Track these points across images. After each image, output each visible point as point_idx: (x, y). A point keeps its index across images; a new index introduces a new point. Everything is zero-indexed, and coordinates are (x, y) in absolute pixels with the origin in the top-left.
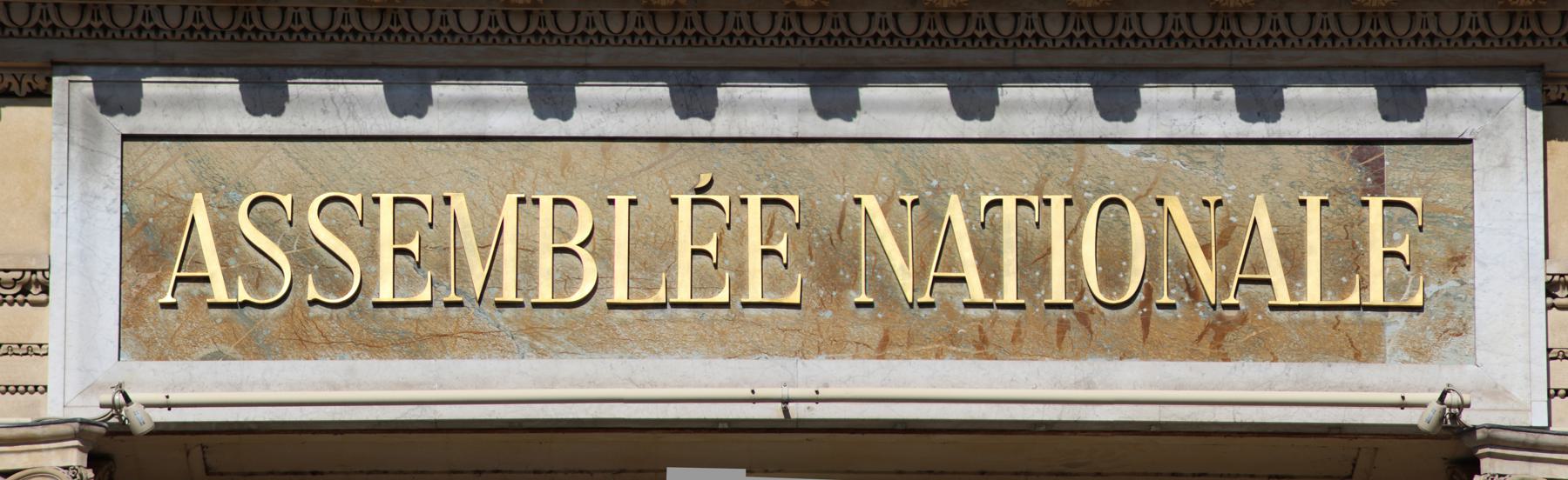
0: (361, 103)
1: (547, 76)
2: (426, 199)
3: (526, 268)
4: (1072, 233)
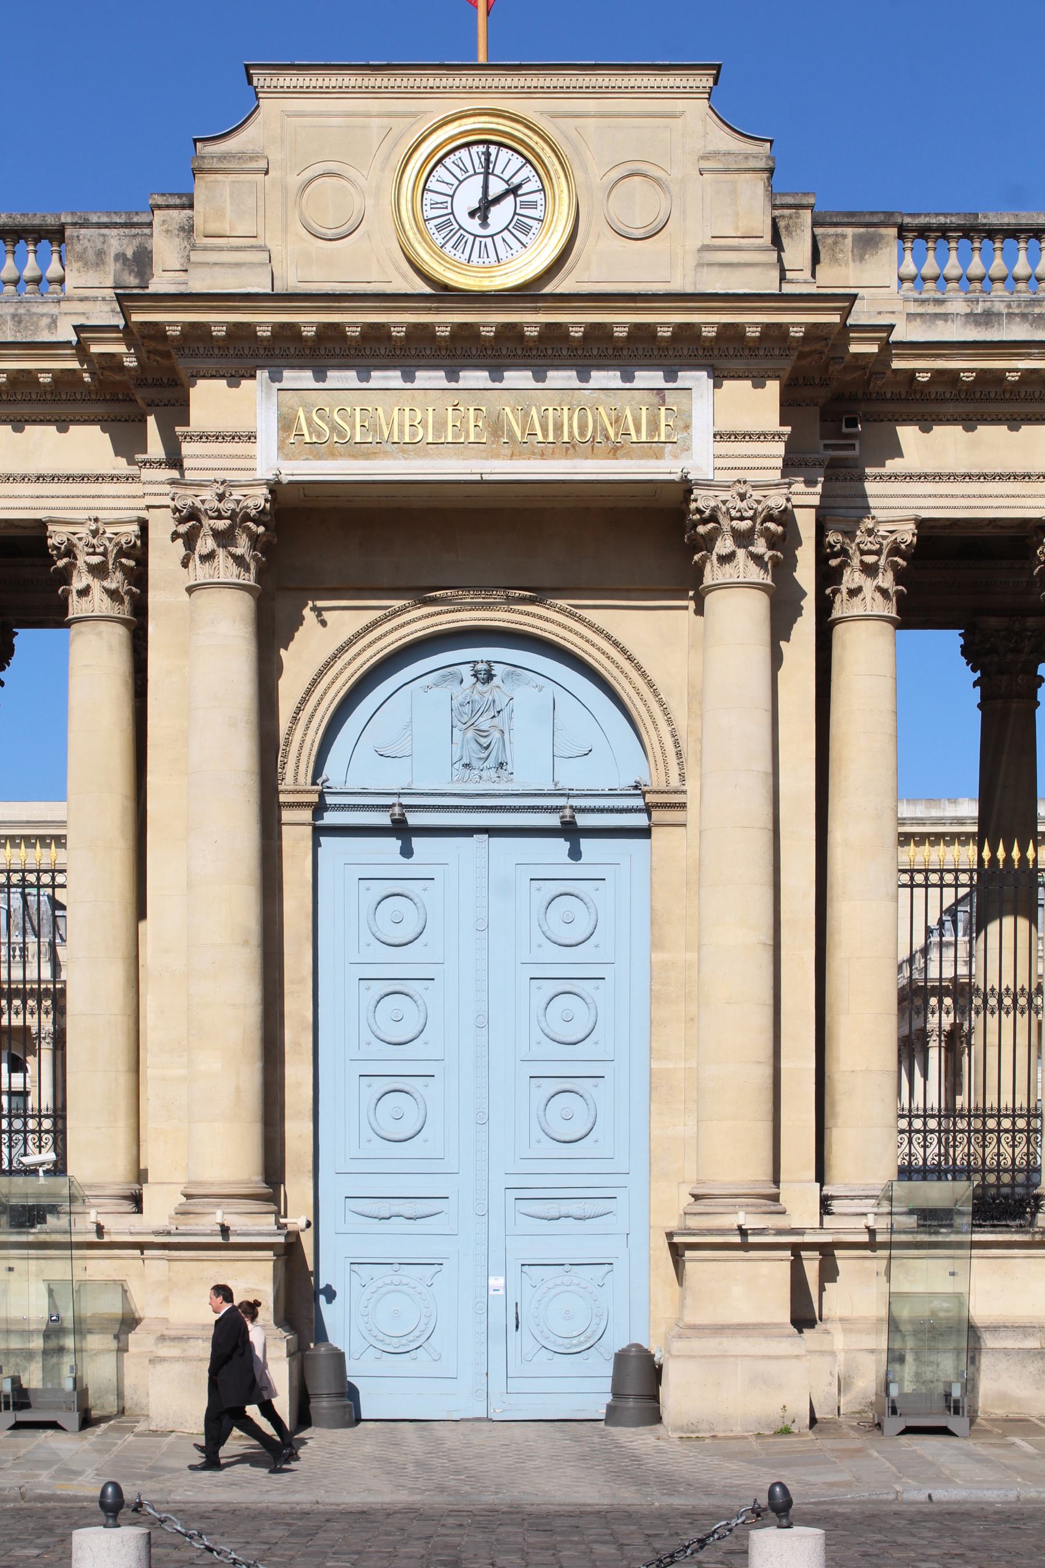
0: (348, 378)
1: (407, 369)
2: (370, 409)
3: (401, 431)
4: (570, 419)
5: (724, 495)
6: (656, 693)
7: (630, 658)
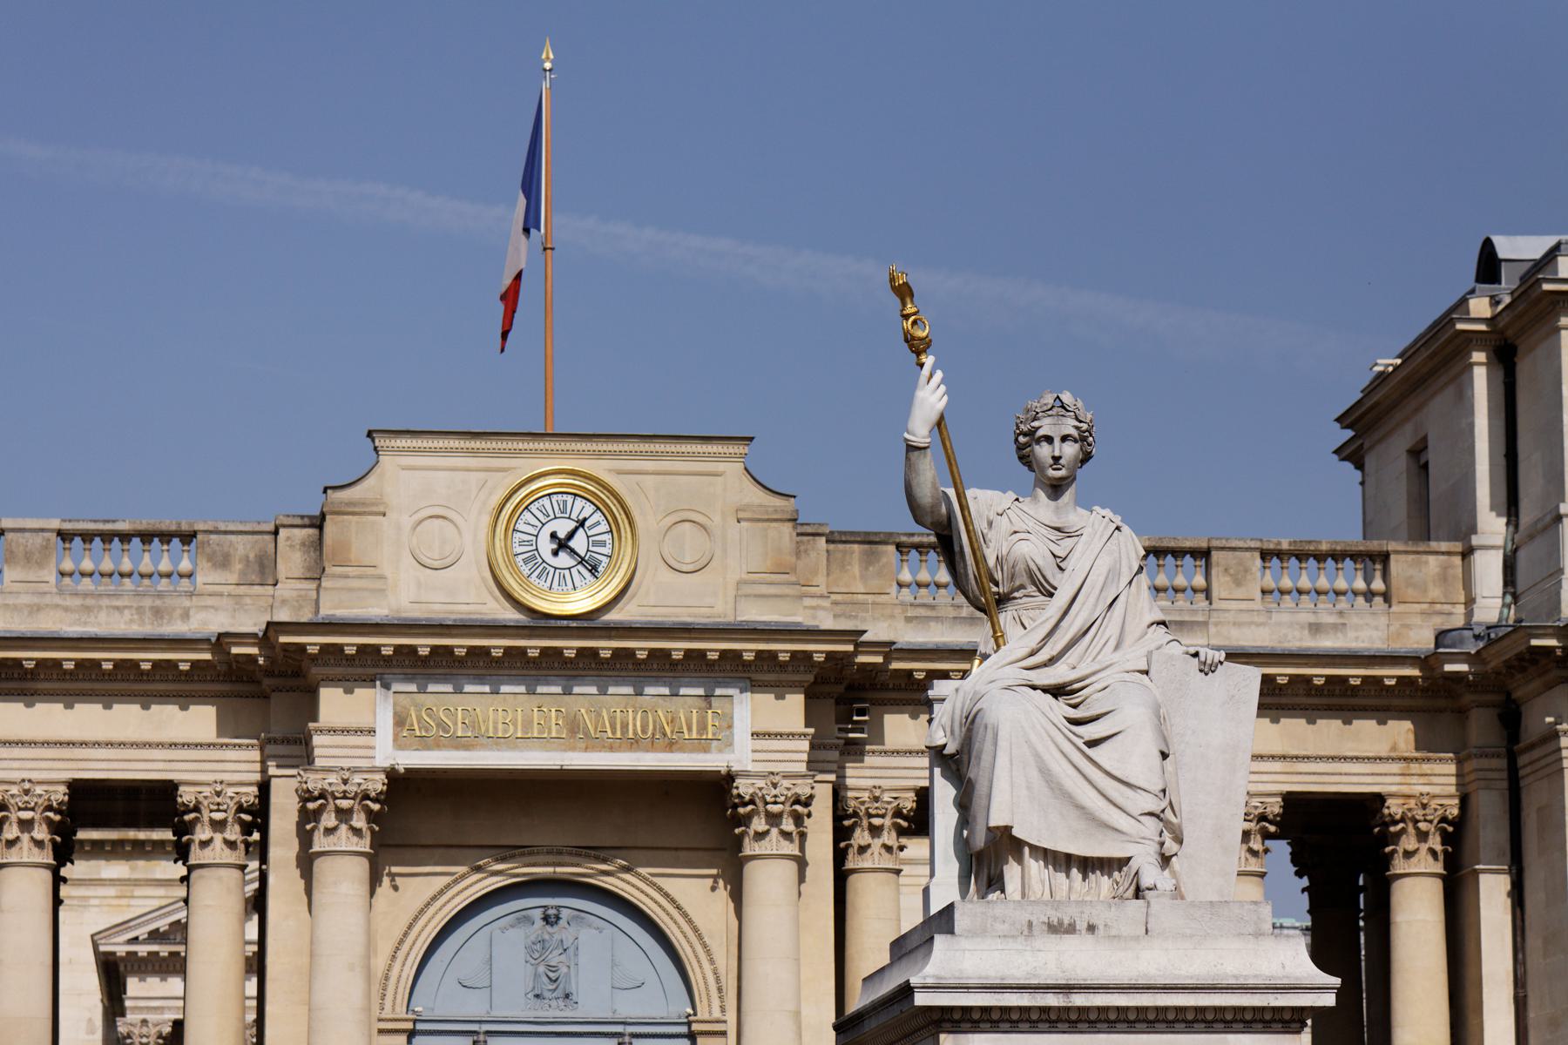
3: (496, 729)
5: (761, 783)
6: (700, 937)
7: (678, 908)
